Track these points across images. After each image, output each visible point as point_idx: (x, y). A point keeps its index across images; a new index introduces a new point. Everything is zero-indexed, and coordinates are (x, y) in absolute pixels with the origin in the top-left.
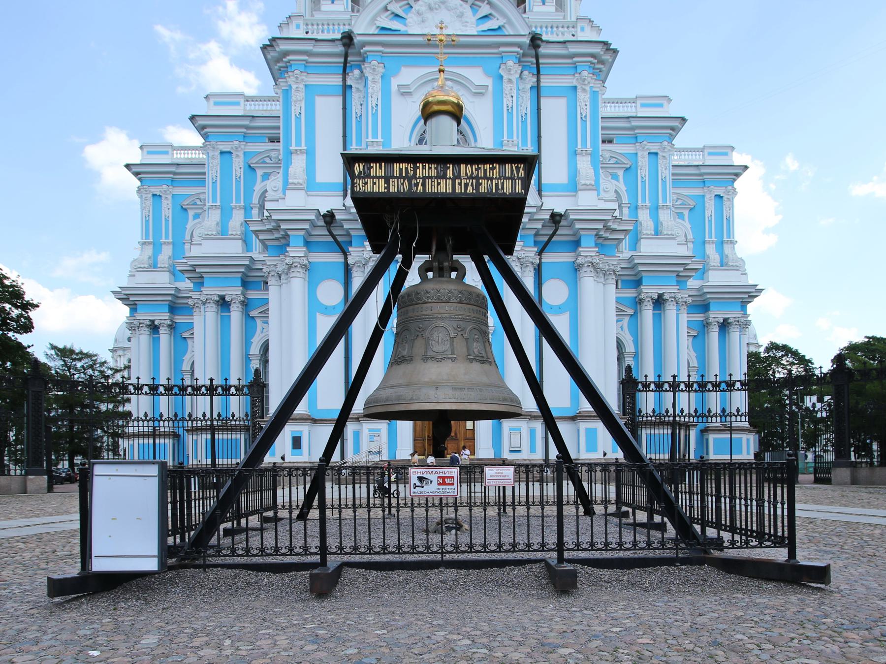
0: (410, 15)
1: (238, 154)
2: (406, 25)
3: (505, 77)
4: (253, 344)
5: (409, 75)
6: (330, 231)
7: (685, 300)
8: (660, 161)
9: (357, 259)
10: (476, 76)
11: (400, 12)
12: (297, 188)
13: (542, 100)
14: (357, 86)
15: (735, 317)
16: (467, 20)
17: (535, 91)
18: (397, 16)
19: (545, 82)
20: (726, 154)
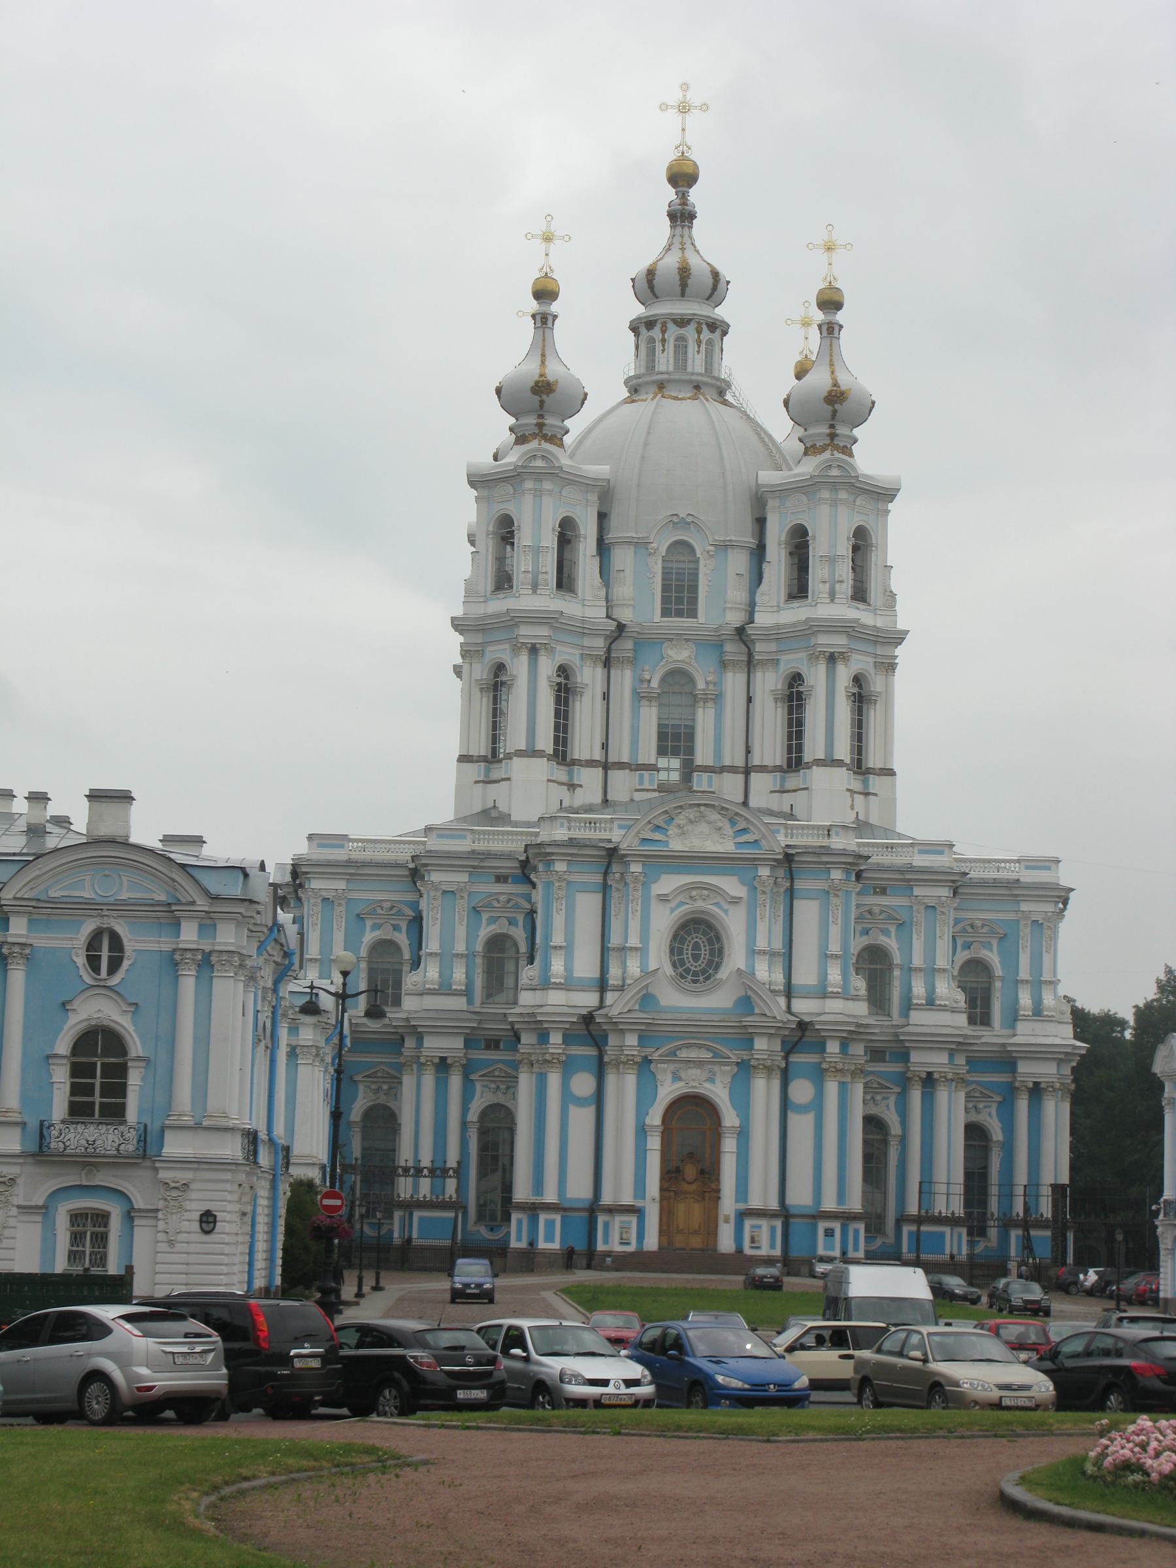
0: (671, 827)
1: (462, 894)
2: (667, 836)
3: (760, 888)
4: (470, 1111)
5: (668, 883)
6: (588, 1031)
7: (962, 1076)
8: (938, 917)
9: (613, 1057)
10: (732, 886)
11: (662, 824)
12: (558, 987)
13: (796, 903)
14: (617, 886)
15: (1047, 1082)
16: (725, 833)
17: (789, 894)
18: (658, 827)
19: (799, 885)
20: (1049, 868)
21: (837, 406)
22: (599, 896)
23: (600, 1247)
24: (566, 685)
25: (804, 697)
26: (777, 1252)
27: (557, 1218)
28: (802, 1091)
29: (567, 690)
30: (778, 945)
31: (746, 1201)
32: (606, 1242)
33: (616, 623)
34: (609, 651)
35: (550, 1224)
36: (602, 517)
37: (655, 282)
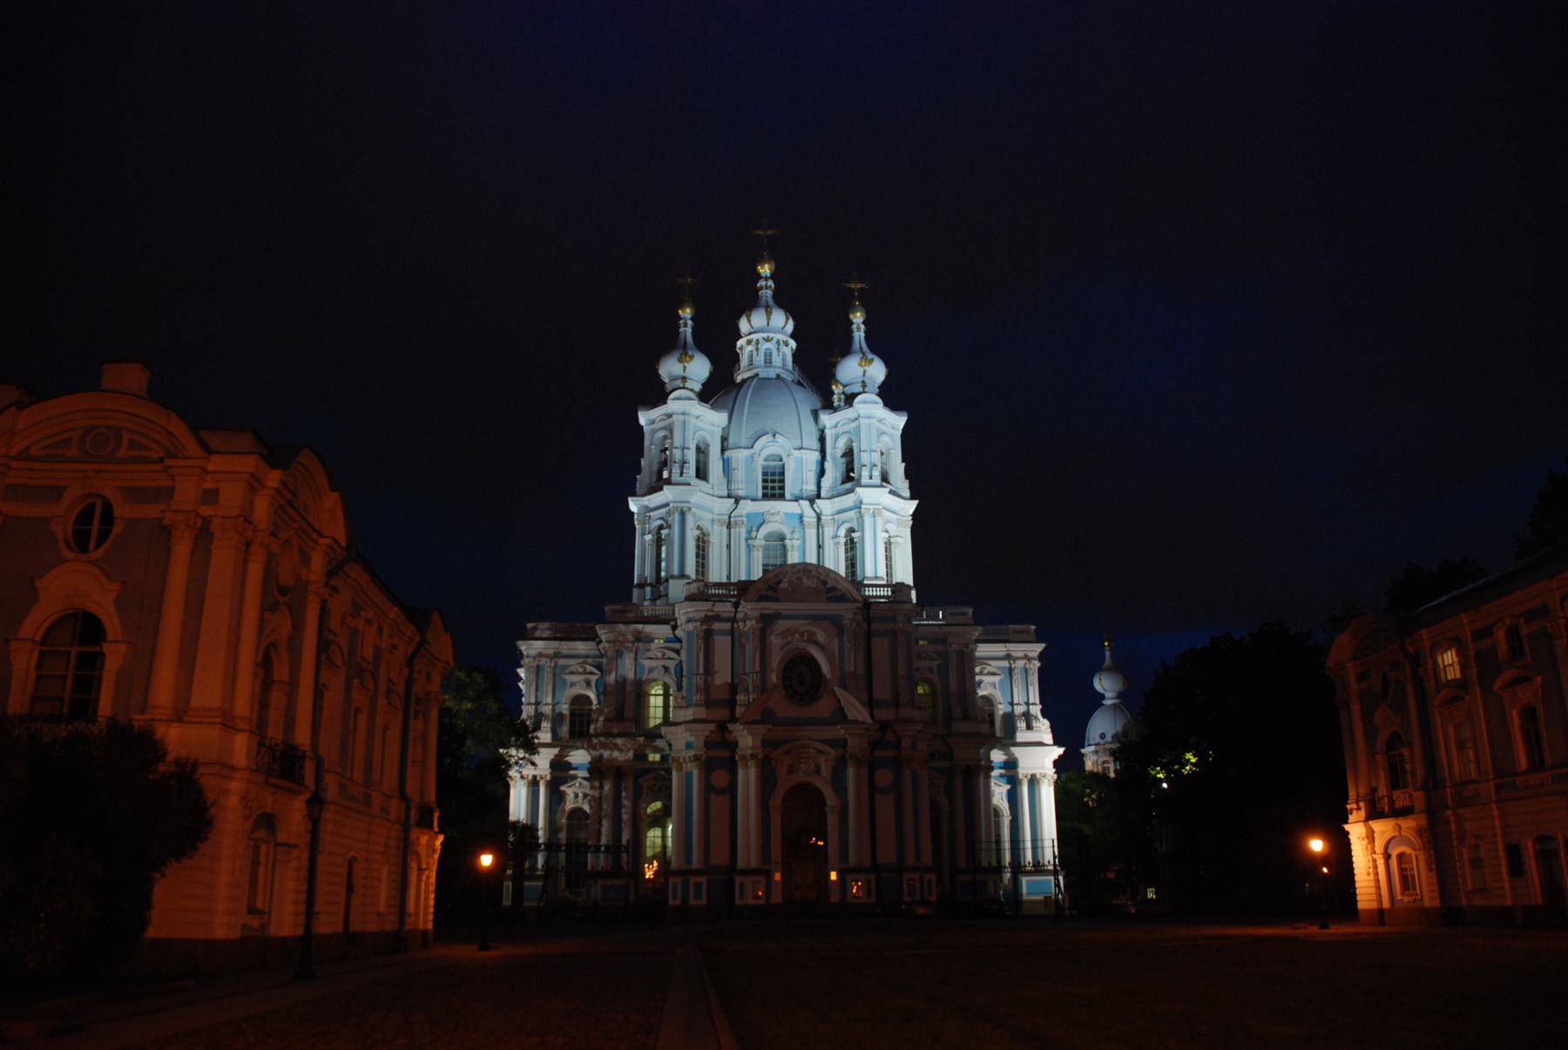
13: (873, 639)
21: (866, 368)
22: (729, 638)
23: (738, 902)
24: (703, 539)
25: (855, 540)
26: (873, 899)
27: (703, 880)
28: (884, 777)
29: (704, 542)
30: (861, 670)
31: (847, 862)
32: (742, 898)
33: (733, 500)
34: (730, 517)
35: (698, 886)
36: (724, 439)
37: (752, 318)
